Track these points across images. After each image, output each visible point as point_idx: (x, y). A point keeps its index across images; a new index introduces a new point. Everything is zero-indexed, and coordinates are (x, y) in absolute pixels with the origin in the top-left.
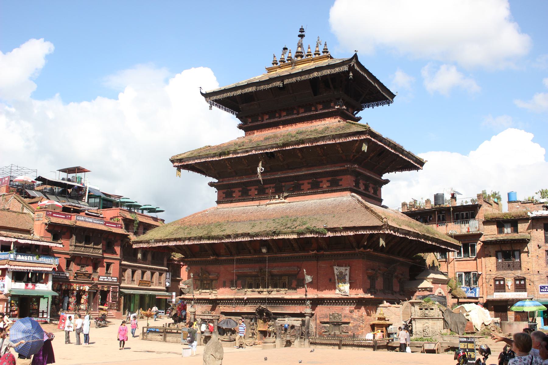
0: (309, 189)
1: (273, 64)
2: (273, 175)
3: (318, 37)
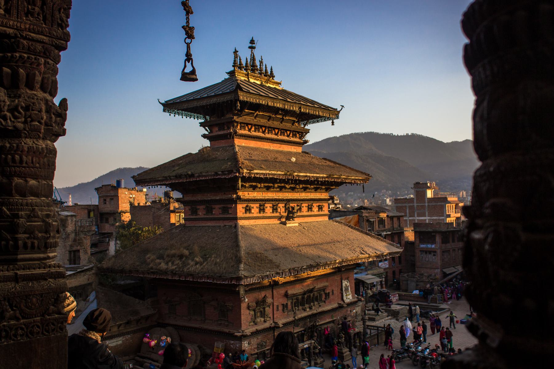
1: (233, 66)
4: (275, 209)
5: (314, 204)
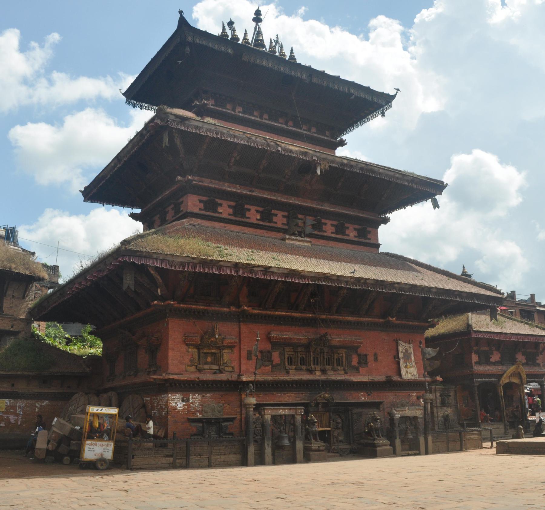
0: (332, 233)
2: (287, 199)
3: (277, 35)
4: (267, 216)
5: (347, 225)
